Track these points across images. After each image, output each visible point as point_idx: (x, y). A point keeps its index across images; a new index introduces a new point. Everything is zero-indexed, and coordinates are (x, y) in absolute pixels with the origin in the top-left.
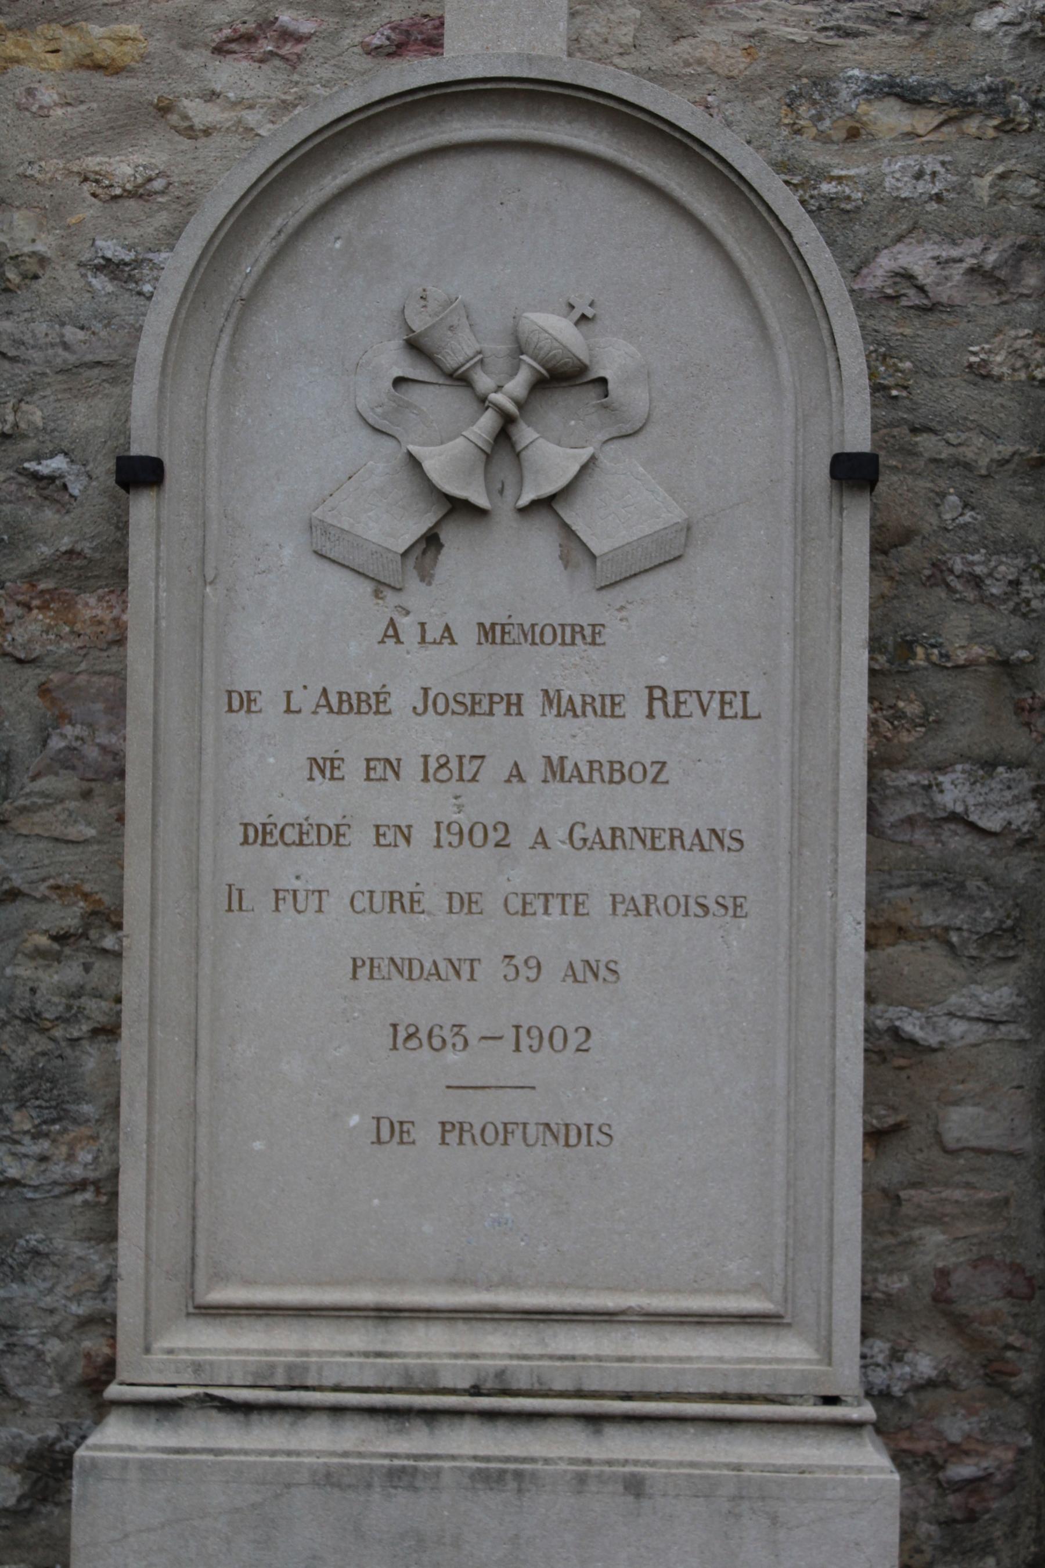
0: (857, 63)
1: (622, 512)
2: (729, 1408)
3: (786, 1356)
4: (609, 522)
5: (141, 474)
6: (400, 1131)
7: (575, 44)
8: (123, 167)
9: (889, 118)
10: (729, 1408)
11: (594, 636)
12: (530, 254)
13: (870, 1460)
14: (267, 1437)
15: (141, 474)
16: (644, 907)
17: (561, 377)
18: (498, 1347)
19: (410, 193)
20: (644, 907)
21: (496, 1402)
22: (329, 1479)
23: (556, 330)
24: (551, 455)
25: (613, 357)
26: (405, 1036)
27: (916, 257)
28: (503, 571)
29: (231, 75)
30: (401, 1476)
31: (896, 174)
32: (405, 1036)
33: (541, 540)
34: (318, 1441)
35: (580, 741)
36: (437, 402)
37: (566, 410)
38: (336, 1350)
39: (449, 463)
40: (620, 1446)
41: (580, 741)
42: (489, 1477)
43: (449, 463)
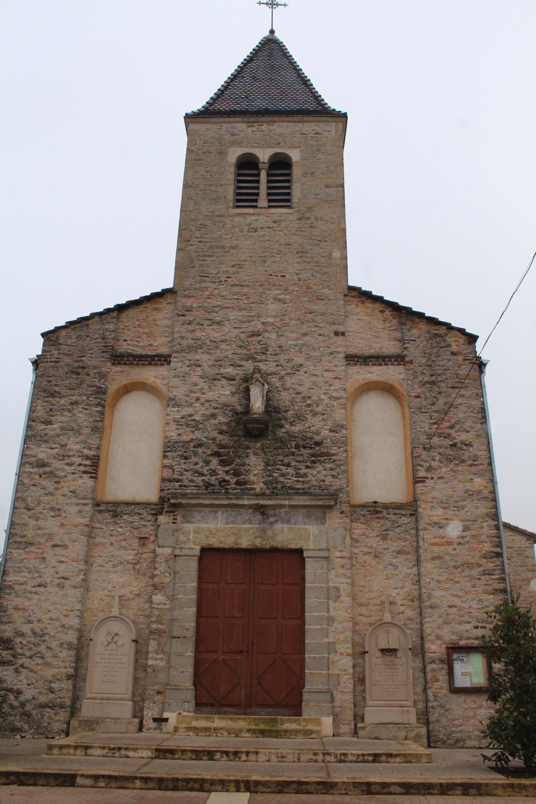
0: (139, 613)
1: (120, 643)
2: (122, 700)
3: (126, 696)
4: (119, 643)
5: (91, 640)
6: (103, 682)
7: (120, 614)
8: (94, 619)
9: (141, 617)
10: (122, 700)
11: (117, 650)
12: (115, 627)
13: (130, 703)
14: (94, 701)
15: (91, 640)
16: (119, 667)
17: (117, 634)
18: (109, 695)
19: (108, 623)
20: (119, 667)
21: (108, 699)
22: (98, 703)
23: (116, 631)
24: (116, 639)
25: (120, 634)
26: (105, 675)
27: (142, 626)
28: (113, 646)
29: (101, 613)
30: (102, 703)
31: (141, 621)
32: (105, 675)
33: (115, 645)
34: (97, 701)
35: (116, 657)
36: (109, 636)
37: (117, 636)
38: (99, 696)
39: (110, 639)
40: (115, 702)
41: (116, 657)
42: (107, 703)
43: (110, 640)
